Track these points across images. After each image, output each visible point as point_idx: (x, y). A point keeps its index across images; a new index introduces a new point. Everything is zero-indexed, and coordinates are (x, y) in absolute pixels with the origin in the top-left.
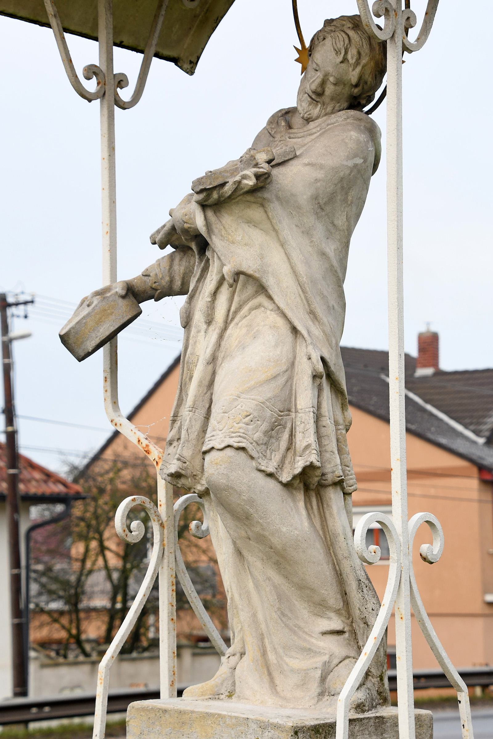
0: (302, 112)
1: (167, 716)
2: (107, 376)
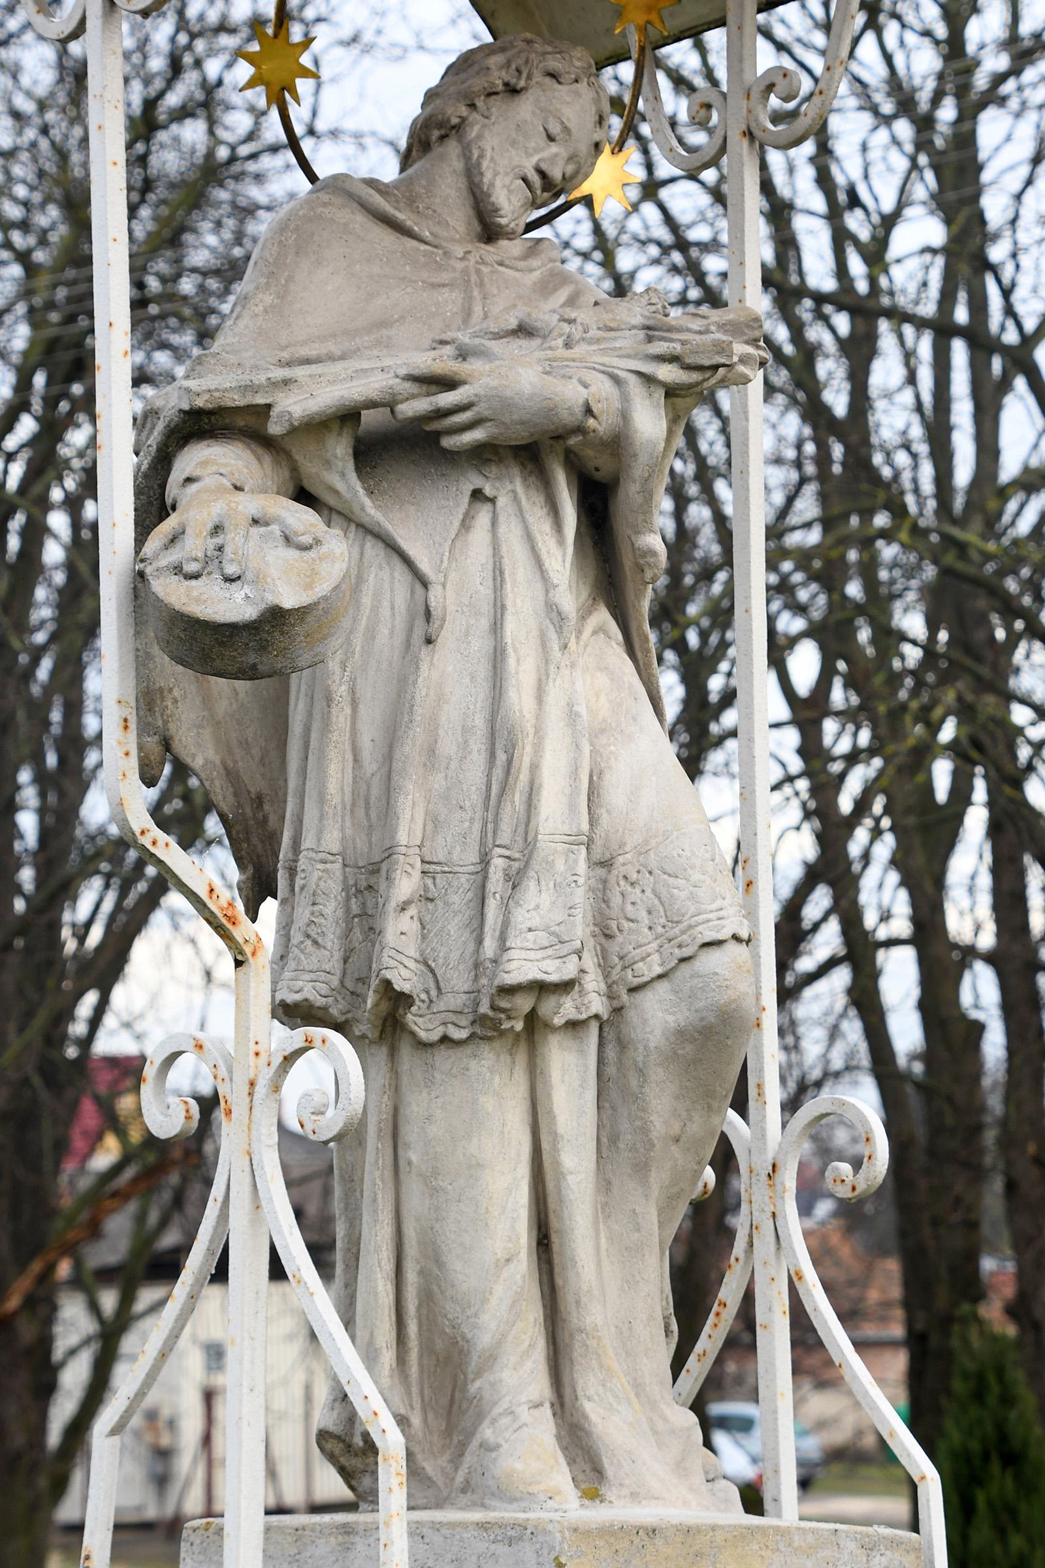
0: (510, 216)
1: (659, 1541)
2: (129, 718)
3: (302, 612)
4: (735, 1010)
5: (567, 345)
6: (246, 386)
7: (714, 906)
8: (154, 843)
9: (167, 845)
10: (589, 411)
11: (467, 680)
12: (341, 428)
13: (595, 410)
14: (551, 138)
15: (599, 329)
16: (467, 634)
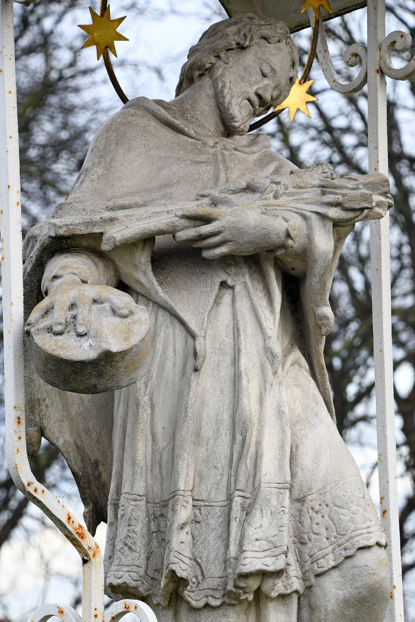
0: (241, 121)
2: (21, 416)
3: (123, 354)
4: (379, 588)
5: (276, 197)
6: (88, 222)
7: (365, 526)
8: (36, 490)
9: (43, 491)
10: (288, 235)
11: (218, 393)
12: (144, 246)
13: (292, 235)
14: (264, 76)
15: (294, 187)
16: (218, 366)
